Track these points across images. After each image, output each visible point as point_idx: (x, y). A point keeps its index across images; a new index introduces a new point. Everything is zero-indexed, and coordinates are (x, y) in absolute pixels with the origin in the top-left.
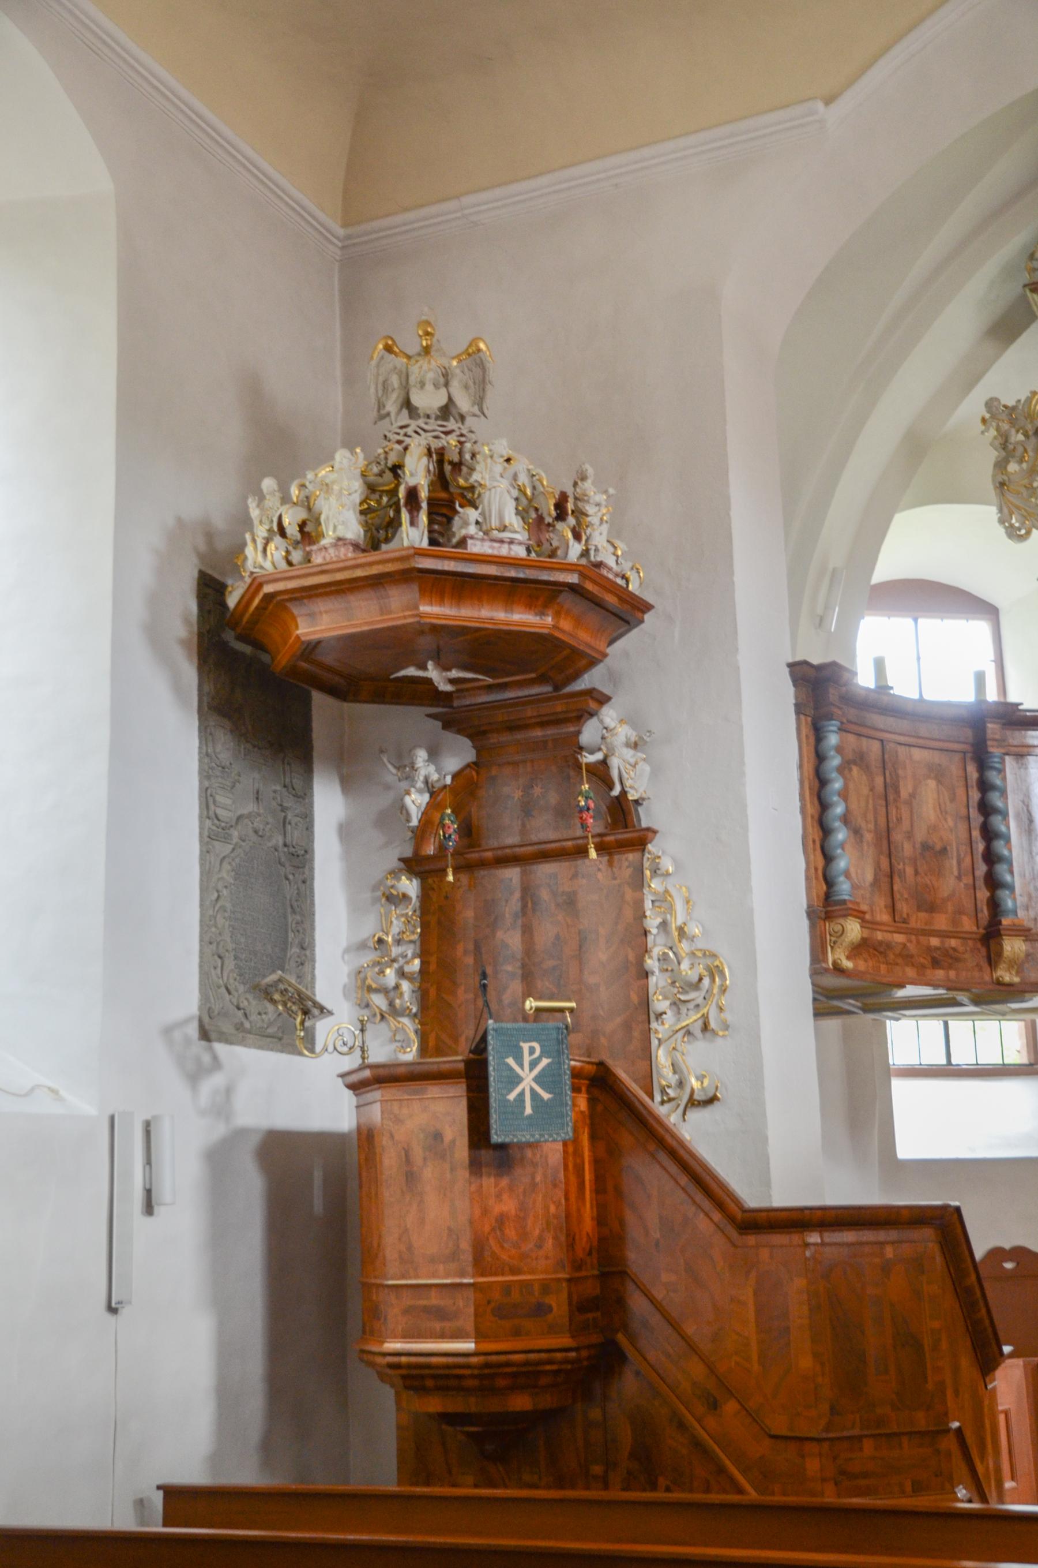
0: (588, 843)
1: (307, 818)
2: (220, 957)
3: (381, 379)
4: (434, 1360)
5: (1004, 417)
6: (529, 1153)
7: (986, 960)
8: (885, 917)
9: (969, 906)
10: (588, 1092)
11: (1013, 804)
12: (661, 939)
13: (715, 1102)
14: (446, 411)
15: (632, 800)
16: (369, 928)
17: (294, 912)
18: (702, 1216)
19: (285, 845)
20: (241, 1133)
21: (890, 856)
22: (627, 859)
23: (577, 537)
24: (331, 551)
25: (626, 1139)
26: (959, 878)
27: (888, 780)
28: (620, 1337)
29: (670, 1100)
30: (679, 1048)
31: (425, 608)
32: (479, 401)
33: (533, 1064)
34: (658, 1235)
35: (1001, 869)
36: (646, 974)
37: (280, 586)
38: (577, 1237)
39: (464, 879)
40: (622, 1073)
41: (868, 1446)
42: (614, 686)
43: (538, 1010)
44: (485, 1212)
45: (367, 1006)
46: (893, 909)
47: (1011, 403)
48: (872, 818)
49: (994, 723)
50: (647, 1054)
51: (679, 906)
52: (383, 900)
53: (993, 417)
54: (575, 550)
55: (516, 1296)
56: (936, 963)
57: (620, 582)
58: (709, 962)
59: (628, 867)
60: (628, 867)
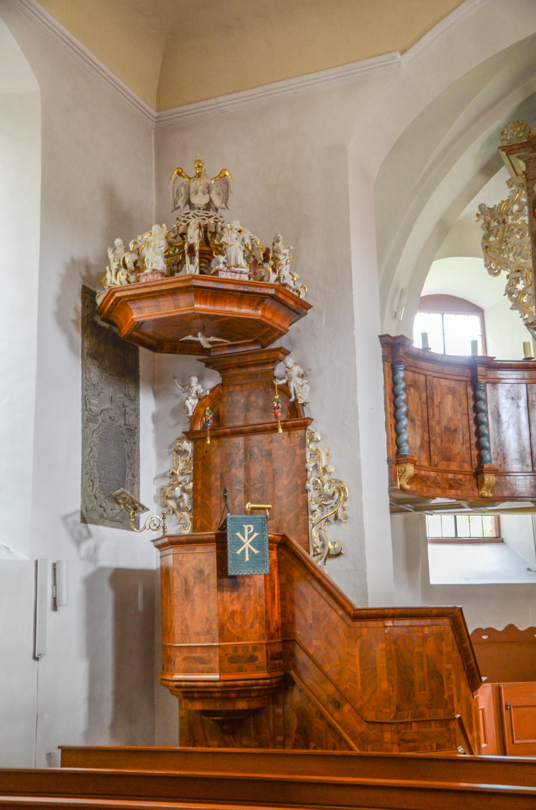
0: (278, 425)
1: (136, 411)
2: (92, 481)
3: (176, 189)
4: (199, 684)
5: (487, 213)
6: (247, 580)
7: (476, 485)
8: (426, 464)
9: (467, 458)
10: (278, 550)
11: (490, 408)
12: (314, 474)
14: (209, 206)
16: (167, 467)
17: (129, 458)
18: (333, 612)
19: (125, 425)
20: (101, 570)
21: (429, 433)
22: (297, 433)
23: (274, 271)
24: (150, 276)
25: (296, 573)
26: (463, 444)
27: (428, 395)
28: (292, 673)
29: (318, 554)
30: (323, 528)
31: (197, 306)
32: (225, 201)
33: (250, 536)
34: (310, 621)
35: (484, 440)
36: (307, 491)
37: (124, 293)
38: (271, 622)
39: (215, 442)
40: (294, 541)
41: (414, 726)
42: (292, 346)
43: (253, 509)
44: (225, 609)
45: (166, 506)
46: (430, 459)
47: (491, 206)
48: (420, 414)
49: (481, 367)
50: (306, 531)
51: (323, 457)
52: (175, 453)
53: (482, 213)
54: (273, 277)
55: (240, 652)
56: (451, 487)
57: (295, 293)
58: (338, 485)
59: (298, 437)
60: (298, 437)
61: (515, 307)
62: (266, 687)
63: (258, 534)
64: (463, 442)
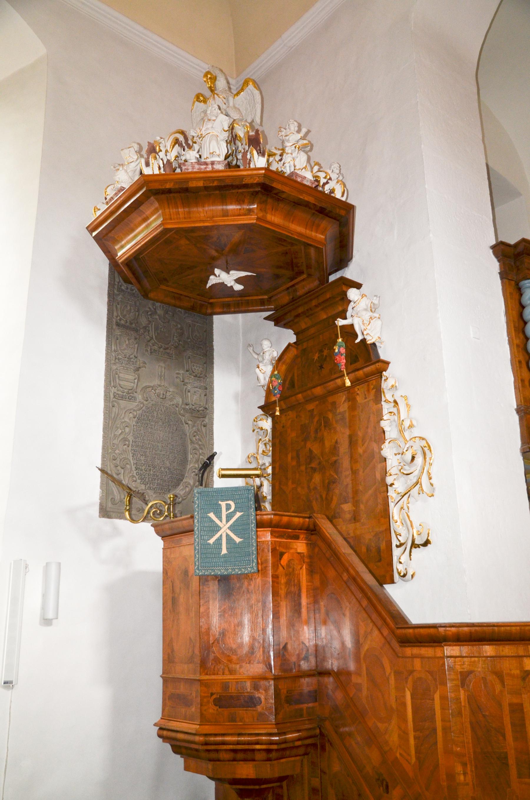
10: (306, 539)
13: (429, 545)
15: (371, 344)
59: (373, 389)
62: (275, 747)
63: (242, 513)
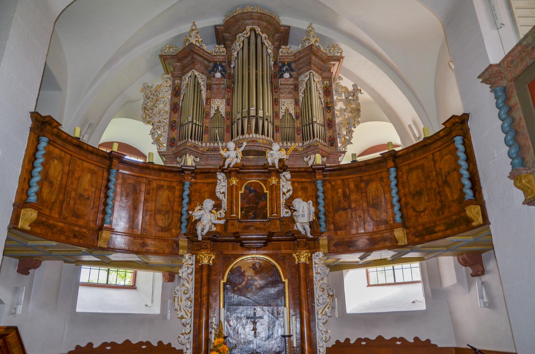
7: (96, 238)
8: (56, 216)
27: (70, 169)
46: (60, 213)
49: (116, 160)
56: (75, 236)
61: (155, 142)
64: (93, 207)
